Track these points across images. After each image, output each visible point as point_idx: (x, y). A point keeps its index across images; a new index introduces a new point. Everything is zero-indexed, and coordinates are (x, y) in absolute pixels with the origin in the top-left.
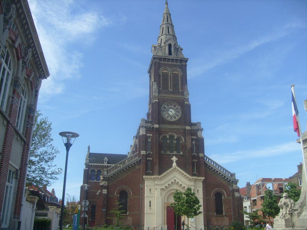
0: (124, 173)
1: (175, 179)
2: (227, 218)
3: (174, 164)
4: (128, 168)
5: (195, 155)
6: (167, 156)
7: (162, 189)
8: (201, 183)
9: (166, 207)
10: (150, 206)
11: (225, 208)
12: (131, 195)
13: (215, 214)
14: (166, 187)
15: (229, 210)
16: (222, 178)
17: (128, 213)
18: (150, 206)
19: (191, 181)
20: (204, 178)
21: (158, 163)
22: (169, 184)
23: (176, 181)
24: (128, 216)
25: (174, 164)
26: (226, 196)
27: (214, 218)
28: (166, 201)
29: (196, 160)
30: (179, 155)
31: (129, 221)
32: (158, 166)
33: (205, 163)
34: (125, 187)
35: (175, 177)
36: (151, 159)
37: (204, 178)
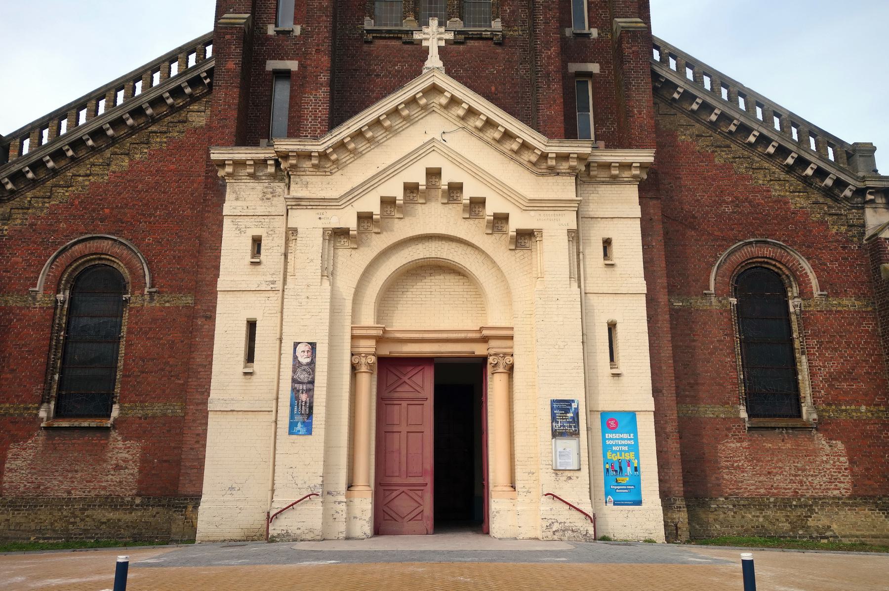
0: (108, 153)
1: (433, 161)
2: (840, 446)
3: (434, 61)
4: (130, 122)
5: (588, 35)
6: (396, 43)
7: (339, 234)
8: (632, 193)
9: (372, 359)
10: (250, 357)
11: (812, 375)
12: (146, 290)
13: (744, 414)
14: (364, 218)
15: (845, 385)
16: (783, 176)
17: (115, 412)
18: (250, 357)
19: (553, 171)
20: (646, 156)
21: (324, 78)
22: (387, 202)
23: (445, 180)
24: (114, 434)
25: (434, 61)
26: (816, 292)
27: (740, 440)
28: (368, 318)
29: (594, 68)
30: (480, 38)
31: (117, 468)
32: (323, 93)
33: (655, 76)
34: (106, 245)
35: (429, 146)
36: (292, 65)
37: (646, 156)
